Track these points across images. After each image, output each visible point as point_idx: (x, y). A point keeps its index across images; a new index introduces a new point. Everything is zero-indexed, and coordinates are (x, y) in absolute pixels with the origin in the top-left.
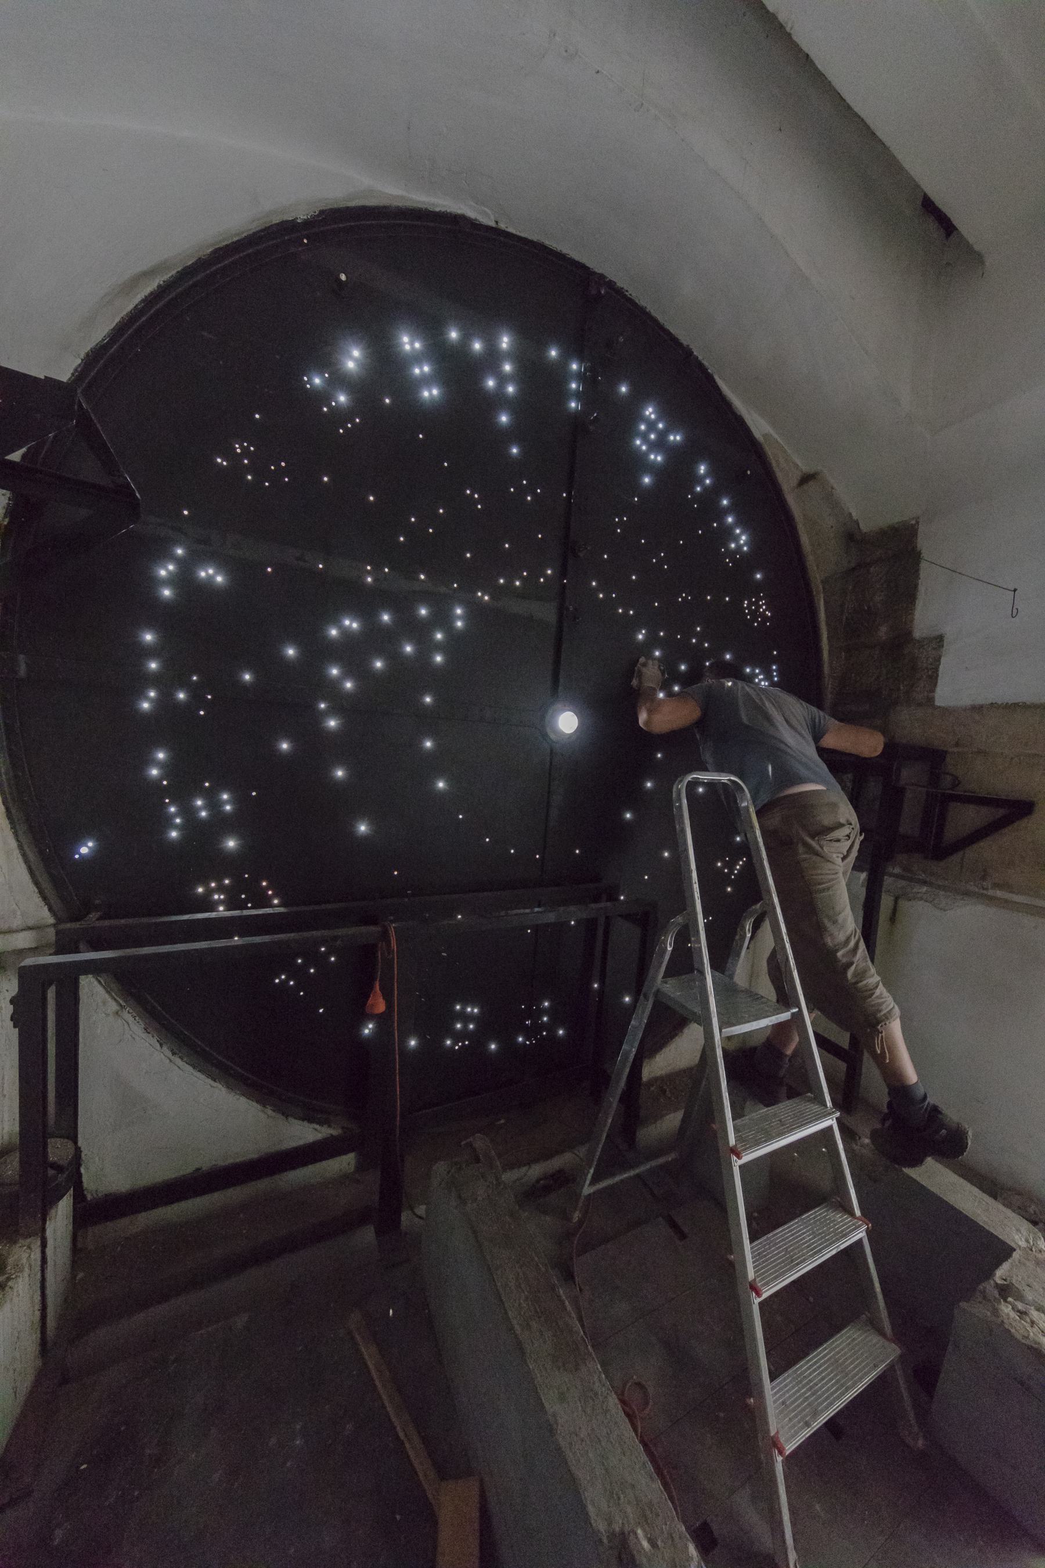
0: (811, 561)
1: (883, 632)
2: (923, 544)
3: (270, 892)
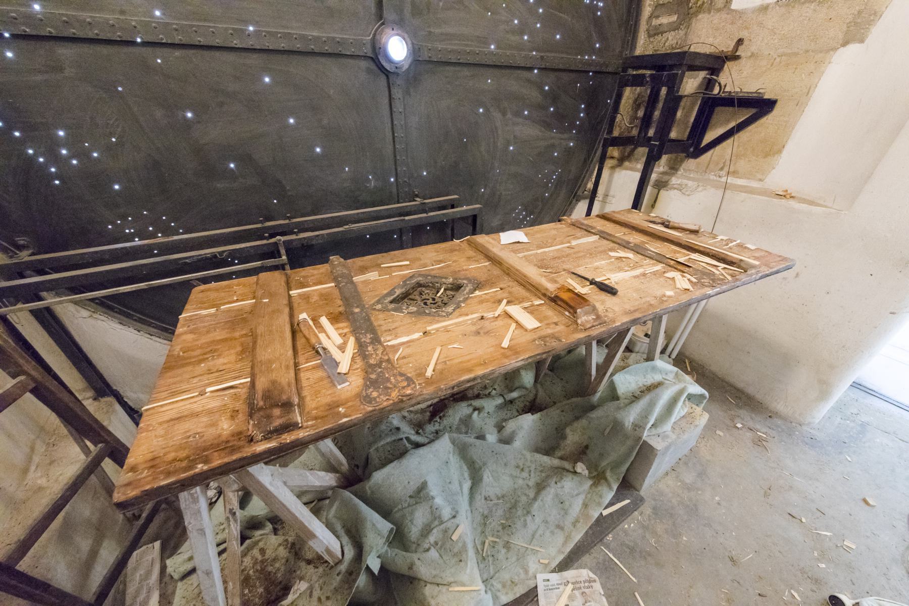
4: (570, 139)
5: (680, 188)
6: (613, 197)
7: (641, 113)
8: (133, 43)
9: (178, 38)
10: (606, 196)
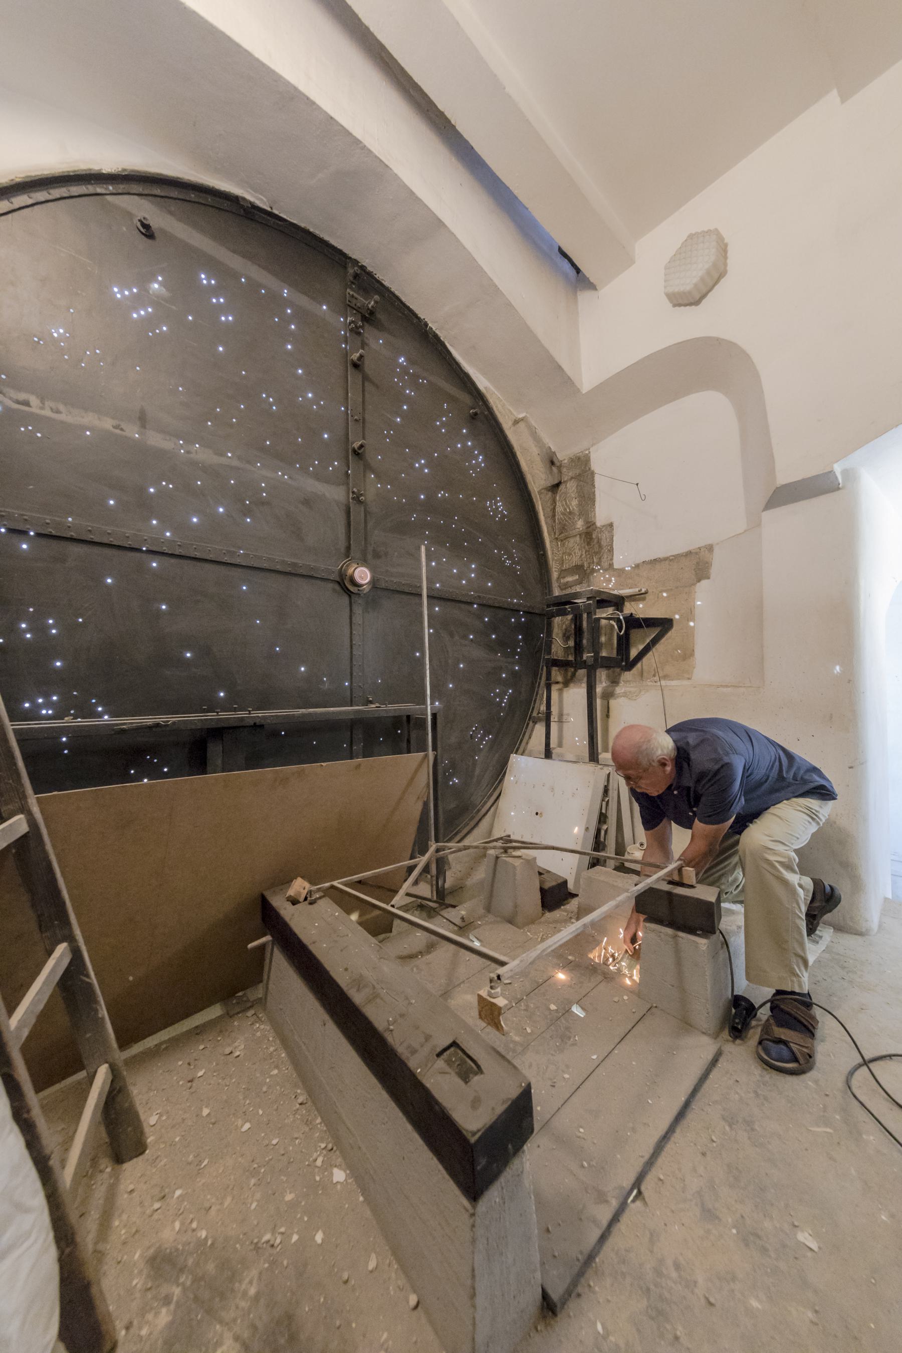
0: (529, 478)
1: (580, 524)
2: (595, 465)
3: (100, 709)
4: (514, 664)
5: (625, 695)
6: (568, 715)
7: (571, 643)
8: (139, 550)
9: (178, 551)
10: (561, 715)
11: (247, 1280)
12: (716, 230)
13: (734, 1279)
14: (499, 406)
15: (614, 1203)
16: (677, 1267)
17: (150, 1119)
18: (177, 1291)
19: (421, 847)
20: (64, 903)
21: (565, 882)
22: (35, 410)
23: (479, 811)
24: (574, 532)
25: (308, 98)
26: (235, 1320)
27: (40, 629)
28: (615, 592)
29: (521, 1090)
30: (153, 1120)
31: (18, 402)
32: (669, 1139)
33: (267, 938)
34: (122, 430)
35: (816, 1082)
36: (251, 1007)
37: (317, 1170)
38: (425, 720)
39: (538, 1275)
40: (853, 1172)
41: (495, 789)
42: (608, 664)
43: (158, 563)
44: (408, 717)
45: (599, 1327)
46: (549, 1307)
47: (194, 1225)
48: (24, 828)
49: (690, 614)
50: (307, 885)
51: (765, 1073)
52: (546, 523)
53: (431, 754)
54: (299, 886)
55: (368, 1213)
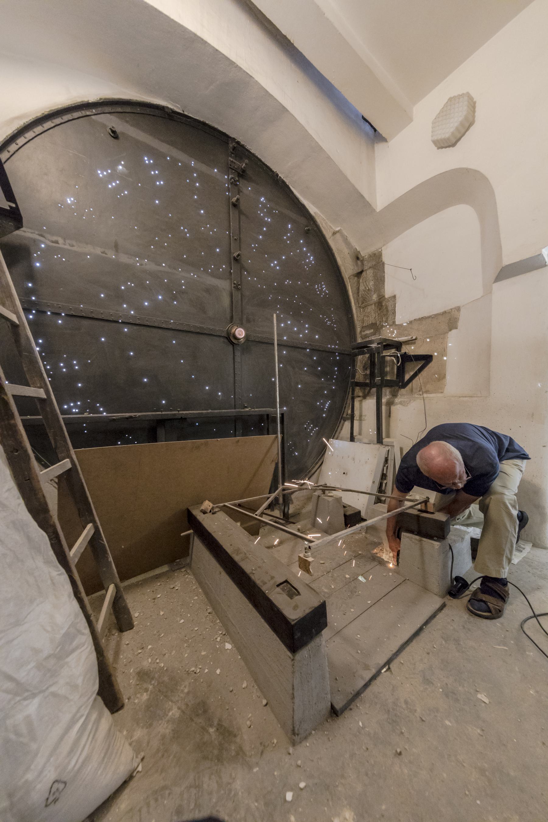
0: (342, 269)
1: (375, 297)
2: (385, 258)
5: (401, 403)
6: (365, 416)
7: (368, 372)
8: (117, 322)
9: (138, 322)
10: (361, 416)
11: (183, 686)
12: (468, 93)
13: (438, 710)
14: (324, 224)
15: (374, 671)
16: (406, 702)
17: (135, 614)
18: (151, 687)
19: (273, 487)
20: (90, 504)
21: (360, 512)
22: (61, 246)
23: (310, 471)
24: (372, 302)
25: (202, 40)
26: (178, 701)
27: (69, 366)
28: (396, 339)
29: (320, 603)
30: (136, 615)
31: (53, 242)
32: (408, 645)
33: (191, 531)
34: (106, 254)
35: (502, 624)
36: (184, 567)
37: (217, 643)
38: (276, 418)
39: (329, 696)
40: (517, 669)
41: (319, 460)
42: (389, 384)
43: (128, 329)
44: (268, 415)
45: (361, 724)
46: (334, 713)
47: (158, 661)
48: (69, 466)
49: (444, 352)
50: (211, 505)
51: (471, 617)
52: (354, 297)
53: (279, 435)
54: (207, 505)
55: (243, 663)
